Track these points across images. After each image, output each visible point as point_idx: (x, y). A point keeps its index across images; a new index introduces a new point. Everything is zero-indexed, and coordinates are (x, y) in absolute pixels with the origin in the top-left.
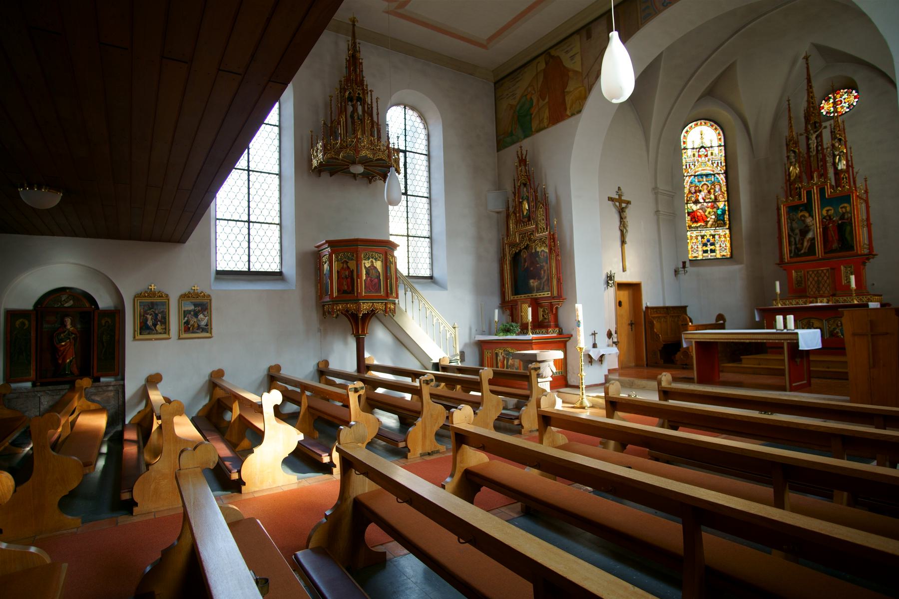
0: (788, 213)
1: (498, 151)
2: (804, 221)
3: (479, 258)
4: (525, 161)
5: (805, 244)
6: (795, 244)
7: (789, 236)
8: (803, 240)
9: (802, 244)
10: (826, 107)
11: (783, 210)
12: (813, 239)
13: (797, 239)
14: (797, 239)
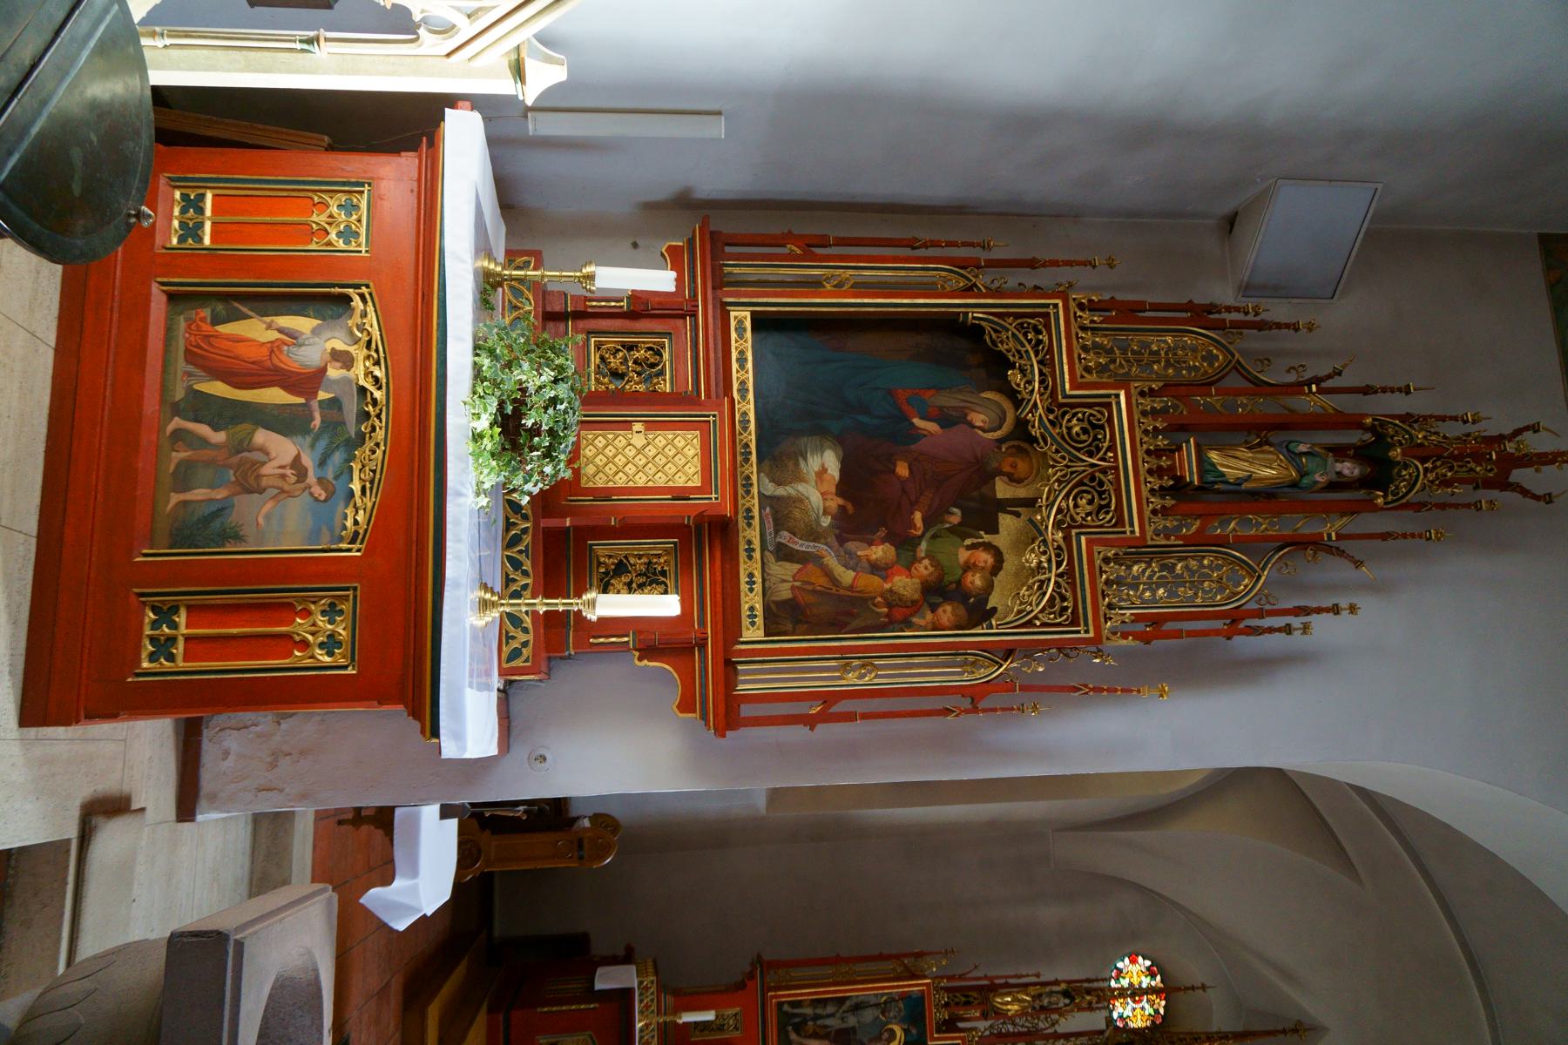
0: (905, 997)
1: (1544, 239)
3: (1022, 123)
4: (1503, 484)
6: (816, 1017)
7: (841, 1001)
10: (1135, 969)
11: (914, 987)
13: (828, 1022)
14: (828, 1022)
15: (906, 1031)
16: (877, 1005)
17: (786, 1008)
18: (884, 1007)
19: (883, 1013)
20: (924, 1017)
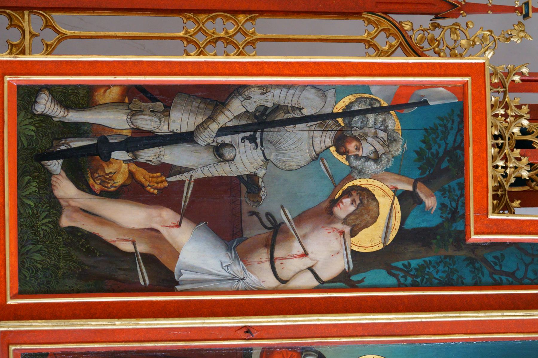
2: (324, 214)
5: (131, 216)
7: (215, 98)
8: (167, 198)
9: (132, 192)
12: (165, 280)
13: (173, 155)
15: (408, 200)
16: (320, 119)
17: (45, 105)
18: (344, 126)
19: (340, 142)
20: (461, 168)
